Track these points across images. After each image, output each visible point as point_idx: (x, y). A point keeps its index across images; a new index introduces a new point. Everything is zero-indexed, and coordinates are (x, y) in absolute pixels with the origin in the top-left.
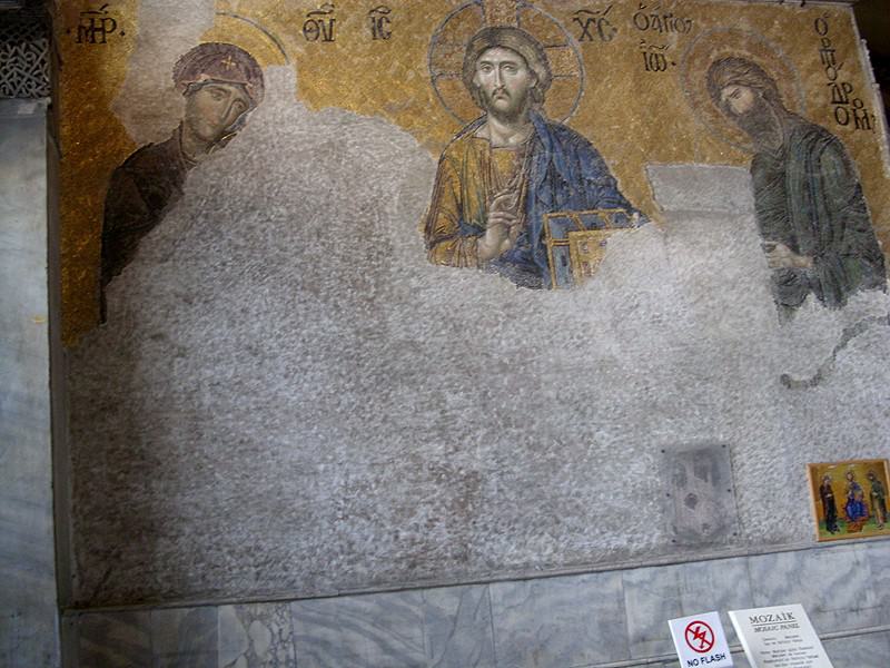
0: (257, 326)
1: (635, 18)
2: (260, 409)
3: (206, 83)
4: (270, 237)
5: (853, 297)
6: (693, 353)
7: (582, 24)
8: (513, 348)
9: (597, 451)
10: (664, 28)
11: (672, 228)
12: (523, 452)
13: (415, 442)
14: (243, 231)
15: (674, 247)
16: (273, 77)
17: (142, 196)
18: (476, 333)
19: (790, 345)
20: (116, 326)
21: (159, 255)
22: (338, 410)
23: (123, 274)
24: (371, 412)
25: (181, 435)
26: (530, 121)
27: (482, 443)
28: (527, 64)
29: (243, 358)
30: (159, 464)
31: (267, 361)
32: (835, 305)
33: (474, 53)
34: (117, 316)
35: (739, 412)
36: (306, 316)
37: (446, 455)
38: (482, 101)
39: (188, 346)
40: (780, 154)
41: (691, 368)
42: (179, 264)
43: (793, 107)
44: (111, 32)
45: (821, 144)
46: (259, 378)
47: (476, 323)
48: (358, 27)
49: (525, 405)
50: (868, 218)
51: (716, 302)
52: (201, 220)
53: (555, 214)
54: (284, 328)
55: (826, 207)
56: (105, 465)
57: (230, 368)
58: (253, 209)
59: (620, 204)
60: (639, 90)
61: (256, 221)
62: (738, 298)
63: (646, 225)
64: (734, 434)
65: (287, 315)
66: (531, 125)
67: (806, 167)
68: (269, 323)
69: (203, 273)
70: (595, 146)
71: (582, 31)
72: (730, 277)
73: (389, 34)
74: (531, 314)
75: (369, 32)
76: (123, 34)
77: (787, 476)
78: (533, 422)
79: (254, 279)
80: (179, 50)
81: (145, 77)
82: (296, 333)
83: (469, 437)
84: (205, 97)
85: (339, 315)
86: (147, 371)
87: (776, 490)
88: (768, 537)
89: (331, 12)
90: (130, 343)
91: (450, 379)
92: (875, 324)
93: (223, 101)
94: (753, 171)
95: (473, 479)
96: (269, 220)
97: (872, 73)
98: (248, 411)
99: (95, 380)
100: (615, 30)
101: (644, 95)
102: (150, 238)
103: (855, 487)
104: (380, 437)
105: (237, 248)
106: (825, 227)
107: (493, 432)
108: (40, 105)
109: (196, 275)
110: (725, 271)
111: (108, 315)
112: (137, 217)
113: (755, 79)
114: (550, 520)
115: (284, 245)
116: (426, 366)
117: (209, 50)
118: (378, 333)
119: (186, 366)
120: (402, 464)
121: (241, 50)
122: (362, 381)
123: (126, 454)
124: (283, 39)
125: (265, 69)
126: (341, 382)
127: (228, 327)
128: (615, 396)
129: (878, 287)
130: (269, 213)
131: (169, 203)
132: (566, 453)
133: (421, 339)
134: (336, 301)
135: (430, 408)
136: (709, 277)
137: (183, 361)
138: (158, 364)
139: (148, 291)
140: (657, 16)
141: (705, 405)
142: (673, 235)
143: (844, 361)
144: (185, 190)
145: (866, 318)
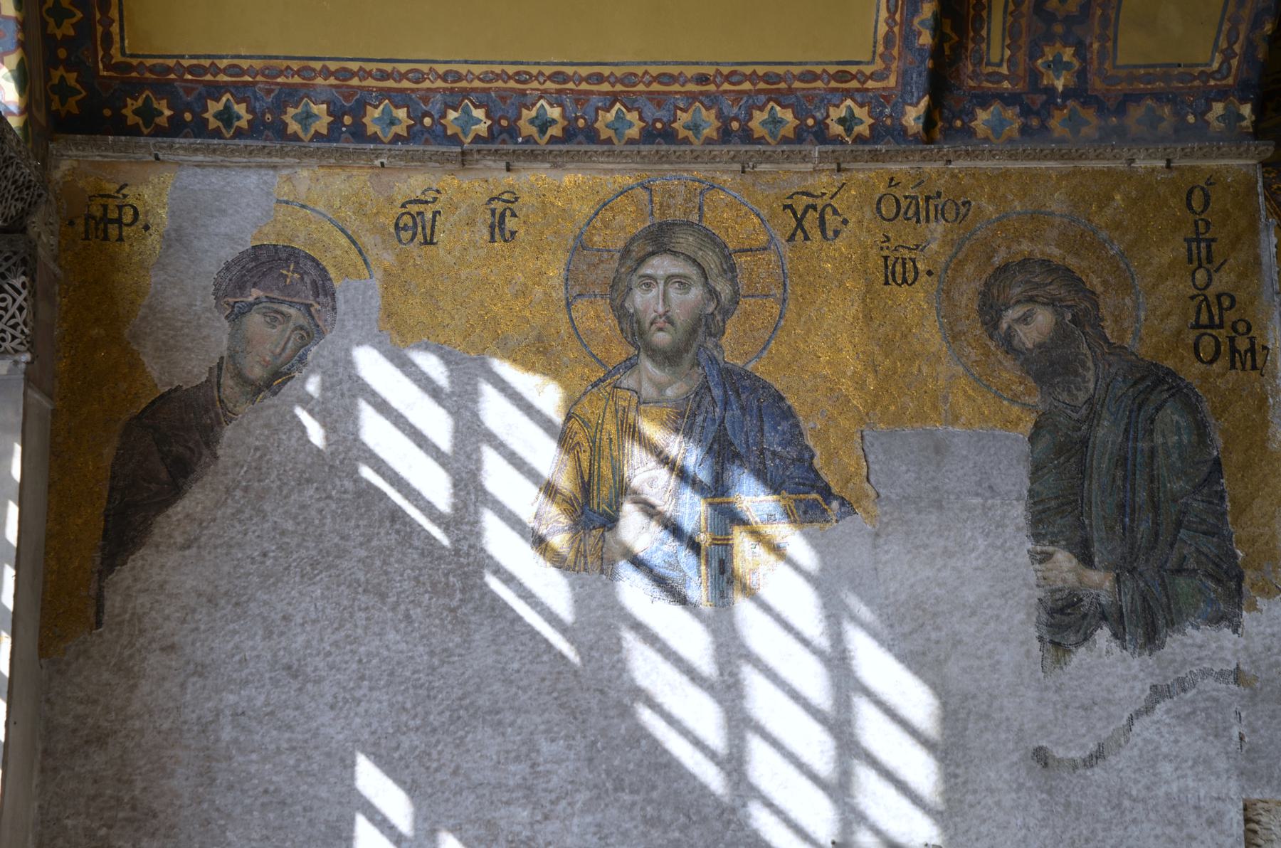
0: (301, 639)
1: (879, 202)
2: (293, 749)
3: (258, 301)
4: (328, 521)
5: (1177, 636)
7: (795, 214)
9: (739, 834)
11: (888, 524)
12: (636, 827)
13: (492, 803)
14: (294, 510)
15: (887, 552)
16: (349, 295)
17: (162, 459)
18: (589, 661)
19: (1055, 704)
20: (115, 633)
21: (180, 540)
22: (396, 755)
23: (129, 565)
24: (438, 760)
25: (187, 779)
26: (699, 365)
27: (583, 812)
28: (706, 278)
29: (280, 680)
30: (155, 816)
31: (309, 686)
32: (1143, 647)
33: (629, 263)
34: (118, 619)
36: (366, 628)
37: (532, 824)
38: (633, 335)
39: (207, 662)
40: (1083, 411)
42: (205, 553)
43: (1121, 338)
44: (129, 225)
45: (1155, 398)
46: (297, 709)
47: (591, 648)
48: (470, 223)
49: (646, 762)
50: (1224, 513)
51: (943, 633)
52: (238, 493)
53: (717, 500)
54: (336, 644)
55: (1151, 495)
56: (83, 816)
57: (260, 693)
58: (309, 481)
59: (813, 487)
60: (869, 318)
61: (311, 497)
62: (978, 631)
65: (341, 626)
67: (1126, 431)
68: (317, 636)
69: (237, 565)
70: (789, 403)
71: (794, 226)
73: (513, 233)
75: (487, 237)
76: (147, 228)
78: (654, 788)
79: (302, 576)
80: (222, 254)
81: (176, 291)
82: (351, 651)
83: (563, 803)
84: (255, 320)
85: (410, 629)
86: (151, 693)
89: (435, 199)
90: (131, 656)
91: (548, 722)
93: (280, 327)
94: (1033, 439)
96: (329, 497)
98: (279, 751)
99: (81, 703)
100: (845, 222)
102: (169, 517)
104: (447, 793)
105: (283, 533)
106: (1144, 528)
107: (599, 797)
108: (16, 363)
109: (226, 568)
111: (106, 618)
112: (153, 486)
115: (347, 531)
116: (517, 704)
117: (264, 257)
118: (460, 655)
119: (204, 687)
121: (308, 257)
122: (432, 717)
123: (113, 803)
124: (364, 239)
125: (338, 284)
126: (404, 718)
127: (264, 639)
130: (330, 487)
131: (198, 469)
132: (696, 833)
133: (516, 666)
134: (407, 610)
135: (517, 759)
137: (200, 683)
138: (167, 685)
139: (161, 587)
140: (915, 198)
142: (888, 535)
143: (1146, 734)
144: (220, 452)
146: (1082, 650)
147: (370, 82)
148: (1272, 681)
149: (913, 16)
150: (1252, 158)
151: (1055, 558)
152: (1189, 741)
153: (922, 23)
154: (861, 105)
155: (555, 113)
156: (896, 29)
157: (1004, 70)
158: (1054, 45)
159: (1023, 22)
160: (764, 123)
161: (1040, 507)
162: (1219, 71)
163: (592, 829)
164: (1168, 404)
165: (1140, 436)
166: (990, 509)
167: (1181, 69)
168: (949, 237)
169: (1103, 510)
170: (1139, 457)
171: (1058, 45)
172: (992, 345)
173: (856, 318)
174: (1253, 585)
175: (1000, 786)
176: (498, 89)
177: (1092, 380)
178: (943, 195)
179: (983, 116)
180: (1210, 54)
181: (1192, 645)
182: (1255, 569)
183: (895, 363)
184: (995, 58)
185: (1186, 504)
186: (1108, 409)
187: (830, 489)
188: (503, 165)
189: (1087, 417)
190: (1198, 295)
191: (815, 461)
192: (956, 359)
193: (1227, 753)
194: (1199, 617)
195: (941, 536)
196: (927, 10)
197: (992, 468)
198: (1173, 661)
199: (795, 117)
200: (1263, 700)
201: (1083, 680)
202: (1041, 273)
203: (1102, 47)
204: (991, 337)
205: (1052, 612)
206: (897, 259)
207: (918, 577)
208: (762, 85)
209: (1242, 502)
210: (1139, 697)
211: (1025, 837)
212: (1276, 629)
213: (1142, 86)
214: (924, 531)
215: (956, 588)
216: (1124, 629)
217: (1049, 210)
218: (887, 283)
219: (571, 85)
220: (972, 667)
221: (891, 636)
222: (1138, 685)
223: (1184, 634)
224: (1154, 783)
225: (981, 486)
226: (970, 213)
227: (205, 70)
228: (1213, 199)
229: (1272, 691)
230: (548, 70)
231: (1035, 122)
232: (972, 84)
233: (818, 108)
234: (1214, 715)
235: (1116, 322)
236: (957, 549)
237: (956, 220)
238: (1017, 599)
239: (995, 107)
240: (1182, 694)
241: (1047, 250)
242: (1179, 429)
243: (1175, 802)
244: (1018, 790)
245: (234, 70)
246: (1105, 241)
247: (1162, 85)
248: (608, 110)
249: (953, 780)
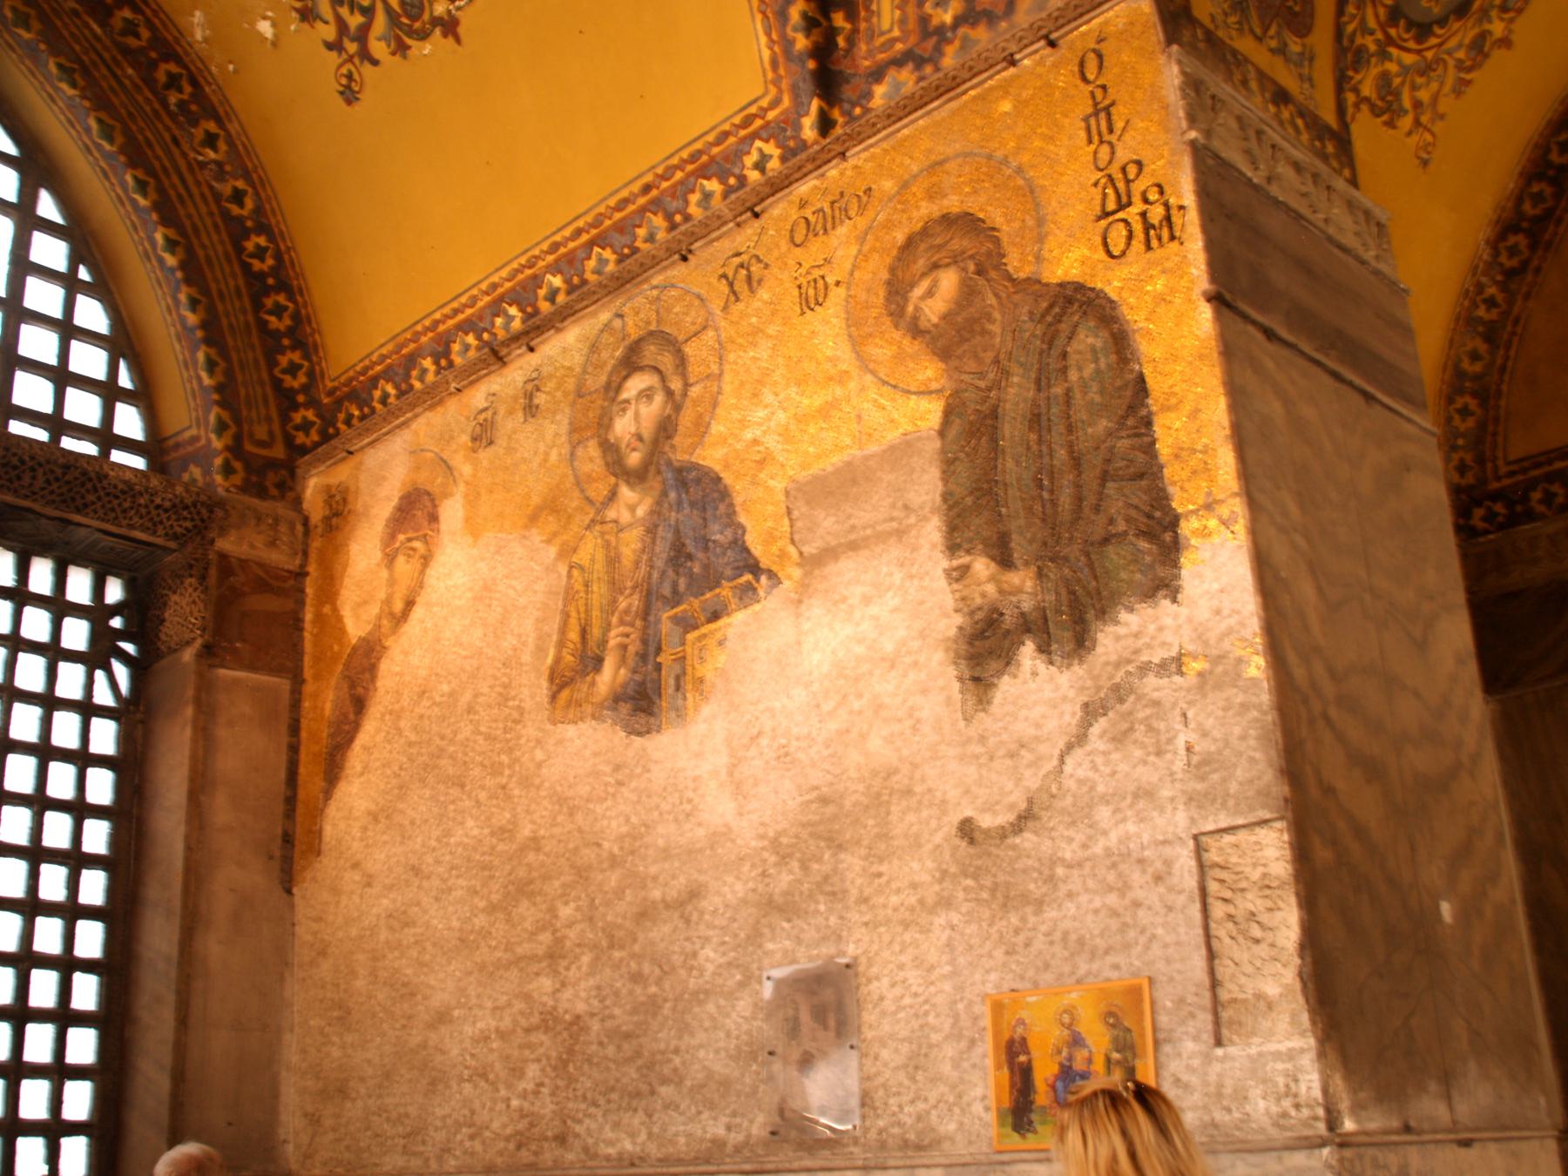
5: (1110, 629)
8: (624, 829)
9: (701, 981)
15: (808, 619)
19: (977, 757)
21: (359, 768)
33: (612, 394)
35: (881, 900)
54: (438, 840)
55: (1071, 452)
64: (872, 942)
66: (659, 478)
67: (1038, 382)
74: (639, 776)
77: (951, 1020)
83: (574, 967)
87: (930, 1046)
88: (912, 1136)
94: (942, 433)
95: (577, 1024)
97: (1181, 114)
103: (1076, 1041)
106: (1065, 499)
113: (965, 243)
114: (644, 1088)
120: (519, 1005)
128: (726, 889)
135: (543, 929)
140: (822, 210)
141: (834, 894)
143: (1081, 773)
145: (1130, 668)
146: (1006, 678)
147: (451, 322)
154: (767, 141)
155: (557, 281)
157: (896, 33)
160: (699, 204)
163: (593, 993)
175: (926, 878)
176: (519, 284)
179: (880, 91)
181: (1126, 636)
184: (886, 25)
188: (524, 348)
198: (1107, 664)
204: (896, 327)
205: (970, 644)
208: (690, 168)
211: (950, 938)
219: (562, 250)
220: (892, 735)
222: (1067, 708)
223: (1117, 623)
224: (1090, 838)
227: (367, 368)
230: (545, 246)
231: (928, 69)
232: (867, 63)
233: (734, 163)
234: (1155, 724)
239: (891, 75)
243: (1115, 858)
244: (941, 881)
245: (383, 358)
248: (589, 258)
249: (877, 881)
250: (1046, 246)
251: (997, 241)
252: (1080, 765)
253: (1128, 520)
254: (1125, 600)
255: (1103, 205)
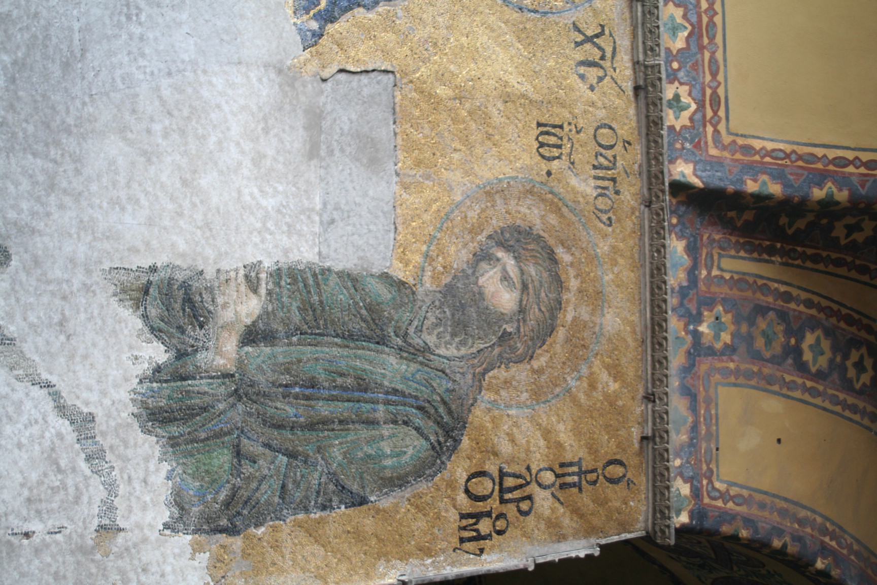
1: (611, 128)
6: (66, 66)
7: (597, 36)
10: (601, 173)
11: (292, 86)
15: (260, 80)
32: (144, 405)
40: (418, 341)
41: (38, 57)
45: (430, 427)
50: (306, 510)
51: (160, 141)
55: (325, 422)
60: (507, 99)
62: (163, 186)
63: (299, 37)
67: (395, 391)
71: (590, 33)
72: (204, 182)
92: (103, 494)
94: (385, 277)
97: (549, 559)
100: (592, 88)
101: (500, 105)
106: (289, 410)
110: (215, 174)
129: (176, 511)
136: (204, 137)
142: (280, 86)
143: (28, 405)
146: (139, 324)
148: (103, 575)
149: (768, 174)
150: (654, 524)
151: (251, 295)
152: (21, 463)
153: (764, 183)
154: (691, 119)
156: (757, 158)
157: (715, 272)
158: (733, 323)
159: (749, 294)
160: (672, 18)
161: (311, 281)
162: (714, 488)
164: (423, 442)
165: (391, 408)
166: (309, 217)
167: (714, 450)
168: (581, 199)
169: (308, 360)
170: (368, 406)
171: (732, 327)
172: (482, 238)
173: (506, 84)
174: (223, 547)
177: (448, 353)
178: (617, 197)
179: (676, 247)
180: (726, 479)
181: (147, 470)
182: (243, 551)
183: (464, 122)
184: (726, 263)
185: (315, 465)
186: (419, 370)
187: (332, 22)
189: (410, 345)
190: (531, 475)
191: (361, 10)
192: (469, 193)
193: (6, 515)
194: (182, 480)
195: (278, 152)
196: (775, 189)
197: (354, 225)
199: (679, 51)
200: (78, 563)
201: (100, 322)
202: (549, 300)
203: (731, 372)
204: (490, 237)
205: (185, 286)
206: (561, 139)
207: (229, 116)
208: (705, 19)
209: (320, 532)
210: (78, 397)
212: (170, 578)
213: (702, 412)
214: (284, 131)
215: (216, 164)
216: (166, 381)
217: (606, 310)
218: (539, 125)
220: (116, 173)
221: (156, 72)
222: (94, 397)
223: (161, 460)
225: (336, 209)
226: (602, 225)
228: (616, 487)
229: (92, 574)
232: (705, 238)
234: (57, 498)
235: (506, 382)
236: (263, 170)
237: (596, 209)
238: (203, 242)
239: (686, 260)
240: (83, 456)
241: (570, 308)
242: (398, 455)
246: (579, 372)
247: (703, 432)
250: (496, 412)
251: (519, 361)
252: (36, 407)
253: (249, 479)
254: (180, 470)
255: (509, 475)
